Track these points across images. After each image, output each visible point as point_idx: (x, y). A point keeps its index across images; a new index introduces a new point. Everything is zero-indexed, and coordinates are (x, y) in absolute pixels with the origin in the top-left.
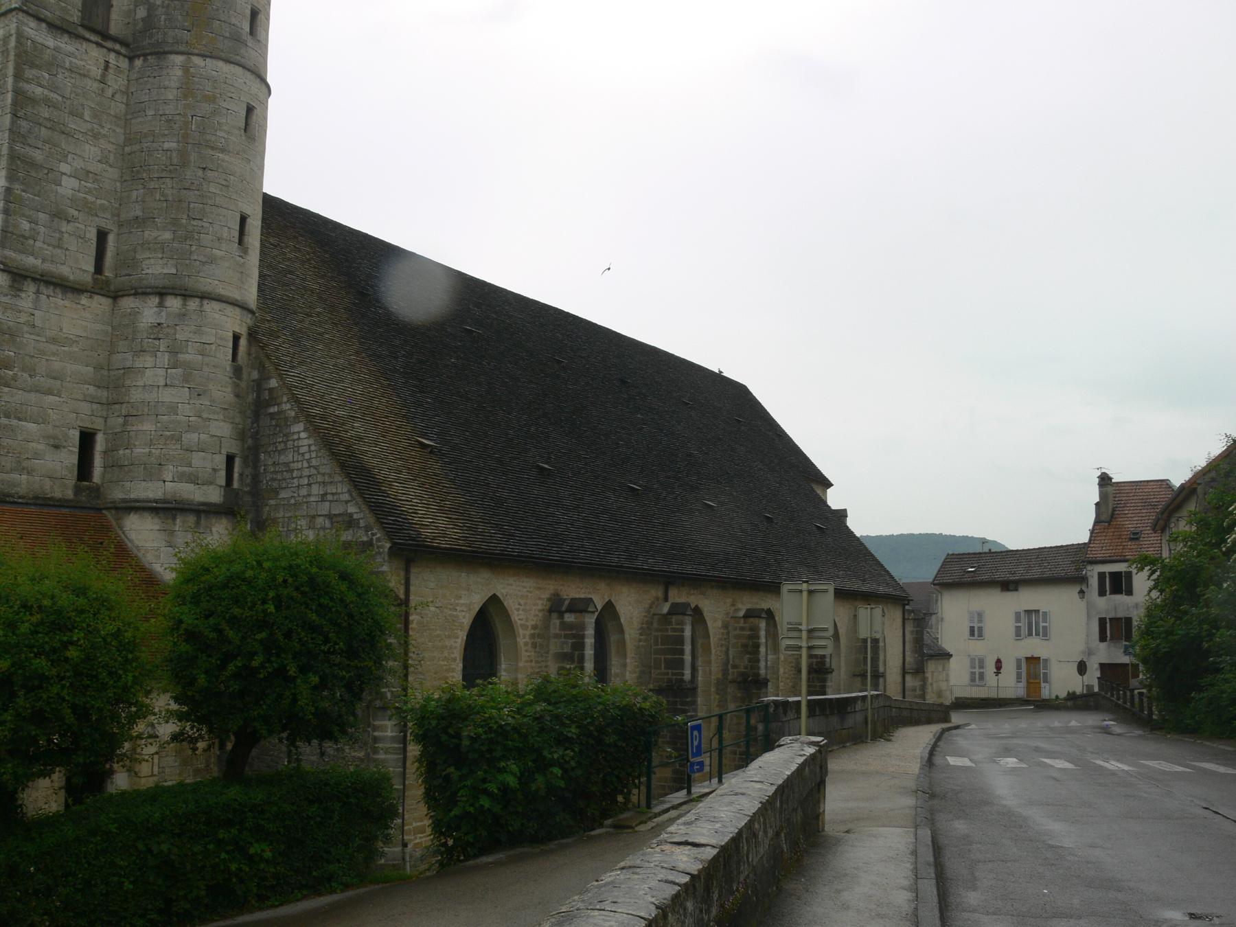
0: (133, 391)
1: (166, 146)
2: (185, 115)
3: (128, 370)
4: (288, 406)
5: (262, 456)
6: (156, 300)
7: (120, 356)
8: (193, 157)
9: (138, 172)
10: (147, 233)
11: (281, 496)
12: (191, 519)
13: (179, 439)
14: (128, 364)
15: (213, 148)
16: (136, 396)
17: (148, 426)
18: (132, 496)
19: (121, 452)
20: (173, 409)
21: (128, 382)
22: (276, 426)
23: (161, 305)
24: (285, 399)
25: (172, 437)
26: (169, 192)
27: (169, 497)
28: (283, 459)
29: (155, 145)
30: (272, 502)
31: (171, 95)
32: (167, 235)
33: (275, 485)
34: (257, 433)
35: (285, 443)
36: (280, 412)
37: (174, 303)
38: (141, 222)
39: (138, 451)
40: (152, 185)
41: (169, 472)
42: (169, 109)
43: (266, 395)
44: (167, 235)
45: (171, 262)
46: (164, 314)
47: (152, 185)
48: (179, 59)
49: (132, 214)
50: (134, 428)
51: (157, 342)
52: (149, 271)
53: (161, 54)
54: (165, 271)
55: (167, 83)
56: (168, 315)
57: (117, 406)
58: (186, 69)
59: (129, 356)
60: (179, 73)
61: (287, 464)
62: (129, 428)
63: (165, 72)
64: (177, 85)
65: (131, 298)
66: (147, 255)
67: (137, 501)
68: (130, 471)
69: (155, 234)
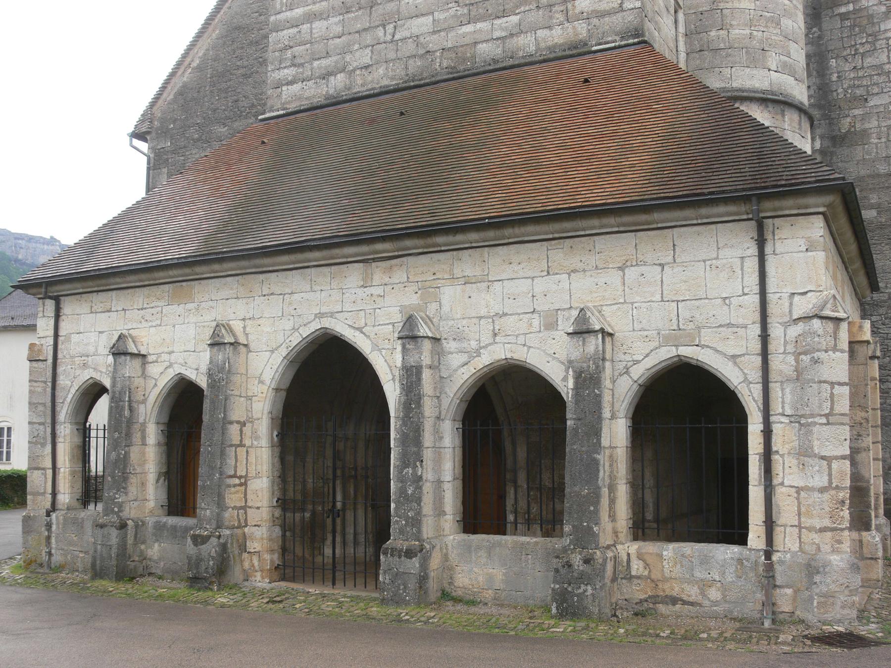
5: (833, 62)
11: (871, 103)
13: (778, 23)
18: (735, 85)
19: (713, 33)
22: (852, 27)
25: (771, 20)
27: (775, 89)
28: (869, 61)
30: (856, 112)
33: (858, 92)
34: (820, 37)
35: (873, 43)
36: (855, 11)
39: (735, 32)
50: (729, 5)
61: (880, 66)
62: (722, 5)
67: (740, 90)
68: (728, 55)
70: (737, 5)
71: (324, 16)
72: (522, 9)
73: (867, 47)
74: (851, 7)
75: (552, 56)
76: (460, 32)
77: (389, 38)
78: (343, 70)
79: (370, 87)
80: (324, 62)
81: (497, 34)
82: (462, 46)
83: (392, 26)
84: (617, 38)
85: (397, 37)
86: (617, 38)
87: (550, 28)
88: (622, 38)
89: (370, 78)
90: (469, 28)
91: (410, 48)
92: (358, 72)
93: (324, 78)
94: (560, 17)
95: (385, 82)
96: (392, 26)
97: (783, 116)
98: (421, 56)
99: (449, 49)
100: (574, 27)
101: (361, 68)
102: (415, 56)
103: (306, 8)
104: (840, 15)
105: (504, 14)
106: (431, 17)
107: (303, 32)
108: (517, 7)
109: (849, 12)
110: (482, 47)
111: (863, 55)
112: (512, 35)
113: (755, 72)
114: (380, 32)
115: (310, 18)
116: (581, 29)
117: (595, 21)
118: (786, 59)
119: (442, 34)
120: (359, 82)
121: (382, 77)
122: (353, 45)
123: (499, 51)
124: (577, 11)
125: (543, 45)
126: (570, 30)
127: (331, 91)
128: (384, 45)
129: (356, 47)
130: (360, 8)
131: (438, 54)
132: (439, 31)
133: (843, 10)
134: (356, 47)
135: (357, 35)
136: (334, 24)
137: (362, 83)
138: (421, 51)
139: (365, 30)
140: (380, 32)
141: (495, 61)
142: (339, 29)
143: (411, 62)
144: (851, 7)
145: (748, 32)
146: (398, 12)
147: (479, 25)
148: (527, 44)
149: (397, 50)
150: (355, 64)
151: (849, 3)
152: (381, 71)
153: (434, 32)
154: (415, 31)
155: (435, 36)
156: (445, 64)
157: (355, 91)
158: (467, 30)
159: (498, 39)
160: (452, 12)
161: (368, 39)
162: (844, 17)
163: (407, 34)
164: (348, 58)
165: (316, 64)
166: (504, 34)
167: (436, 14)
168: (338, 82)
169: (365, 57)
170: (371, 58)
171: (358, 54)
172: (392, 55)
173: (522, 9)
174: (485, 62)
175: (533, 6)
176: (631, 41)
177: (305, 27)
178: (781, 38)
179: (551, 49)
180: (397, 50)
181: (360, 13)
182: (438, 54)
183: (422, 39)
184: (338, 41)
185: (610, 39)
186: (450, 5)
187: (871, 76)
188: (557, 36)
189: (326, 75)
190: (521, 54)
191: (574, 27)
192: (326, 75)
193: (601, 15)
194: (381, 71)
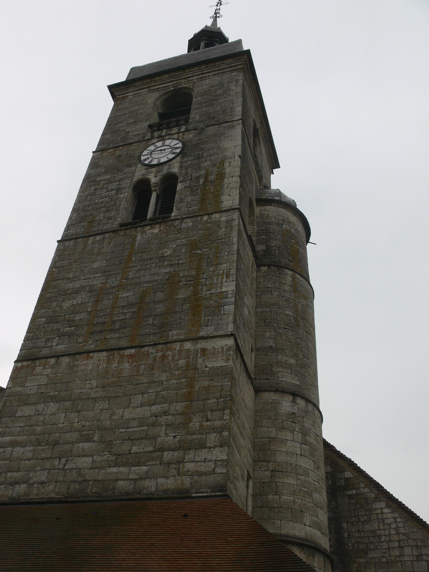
0: (278, 454)
1: (287, 312)
2: (295, 300)
3: (273, 440)
4: (367, 490)
5: (345, 525)
6: (291, 398)
7: (264, 429)
8: (301, 323)
9: (269, 322)
10: (280, 357)
12: (322, 559)
13: (311, 496)
14: (273, 435)
15: (308, 323)
16: (281, 458)
17: (291, 481)
18: (282, 532)
19: (270, 497)
20: (306, 473)
21: (273, 448)
23: (294, 401)
24: (362, 485)
26: (291, 337)
28: (367, 527)
29: (280, 310)
31: (287, 288)
32: (292, 361)
36: (357, 495)
37: (301, 402)
38: (275, 350)
39: (285, 498)
40: (280, 331)
41: (308, 519)
42: (287, 295)
43: (343, 483)
44: (292, 361)
45: (296, 377)
46: (296, 407)
47: (280, 331)
48: (290, 272)
49: (267, 345)
50: (281, 480)
51: (293, 425)
52: (284, 379)
53: (280, 267)
54: (294, 382)
55: (284, 281)
56: (299, 409)
57: (265, 464)
58: (294, 278)
59: (273, 430)
60: (291, 279)
62: (277, 480)
63: (282, 276)
64: (290, 284)
65: (272, 393)
66: (281, 369)
67: (286, 536)
69: (285, 358)
70: (286, 481)
71: (23, 445)
72: (151, 463)
73: (366, 518)
74: (354, 492)
75: (165, 496)
76: (109, 471)
77: (61, 466)
78: (26, 482)
79: (41, 496)
80: (15, 474)
81: (132, 476)
82: (108, 480)
83: (65, 459)
84: (209, 491)
85: (67, 467)
86: (209, 491)
87: (167, 478)
88: (212, 491)
89: (42, 491)
90: (115, 470)
91: (74, 475)
92: (36, 485)
93: (12, 485)
94: (173, 472)
95: (52, 495)
96: (65, 459)
97: (314, 557)
98: (80, 482)
99: (99, 481)
100: (182, 480)
101: (39, 483)
102: (75, 482)
103: (13, 438)
104: (349, 495)
105: (138, 464)
106: (91, 458)
107: (7, 452)
108: (148, 461)
109: (353, 495)
110: (121, 484)
111: (363, 523)
112: (141, 479)
113: (296, 525)
114: (56, 462)
115: (14, 444)
116: (187, 481)
117: (196, 478)
118: (316, 519)
119: (96, 470)
120: (35, 492)
121: (51, 491)
122: (37, 467)
123: (131, 487)
124: (185, 470)
125: (160, 488)
126: (179, 481)
127: (15, 495)
128: (57, 471)
129: (39, 468)
130: (47, 444)
131: (91, 483)
132: (95, 468)
133: (350, 493)
134: (39, 468)
135: (41, 461)
136: (28, 451)
137: (35, 493)
138: (80, 479)
139: (47, 459)
140: (56, 462)
141: (127, 494)
142: (30, 455)
143: (72, 485)
144: (354, 492)
145: (292, 498)
146: (71, 451)
147: (121, 469)
148: (150, 485)
149: (65, 476)
150: (35, 480)
151: (353, 489)
152: (51, 487)
153: (91, 468)
154: (79, 465)
155: (91, 471)
156: (94, 490)
157: (31, 497)
158: (113, 471)
159: (131, 479)
160: (105, 457)
161: (48, 465)
162: (351, 497)
163: (74, 466)
164: (31, 474)
165: (9, 474)
166: (136, 477)
167: (95, 457)
168: (21, 489)
169: (43, 476)
170: (47, 477)
171: (38, 473)
172: (60, 478)
173: (151, 463)
174: (121, 493)
175: (158, 462)
176: (218, 494)
177: (9, 449)
178: (313, 505)
179: (165, 491)
180: (65, 476)
181: (47, 447)
182: (91, 483)
183: (82, 471)
184: (28, 462)
185: (204, 490)
186: (105, 453)
187: (368, 537)
188: (170, 483)
189: (14, 483)
190: (145, 492)
191: (182, 480)
192: (14, 483)
193: (200, 474)
194: (51, 487)
